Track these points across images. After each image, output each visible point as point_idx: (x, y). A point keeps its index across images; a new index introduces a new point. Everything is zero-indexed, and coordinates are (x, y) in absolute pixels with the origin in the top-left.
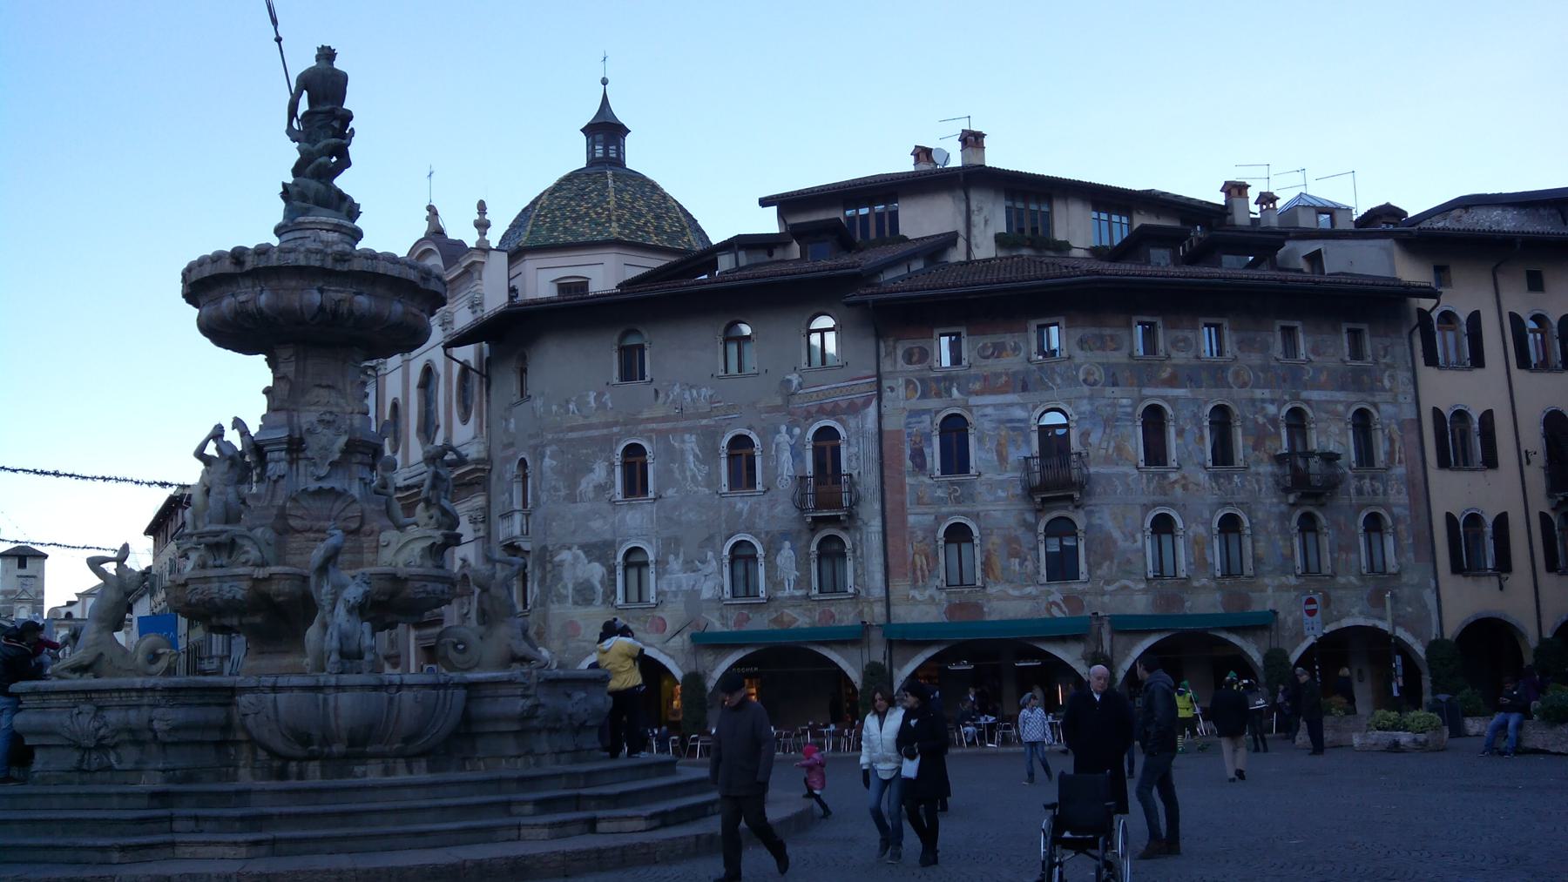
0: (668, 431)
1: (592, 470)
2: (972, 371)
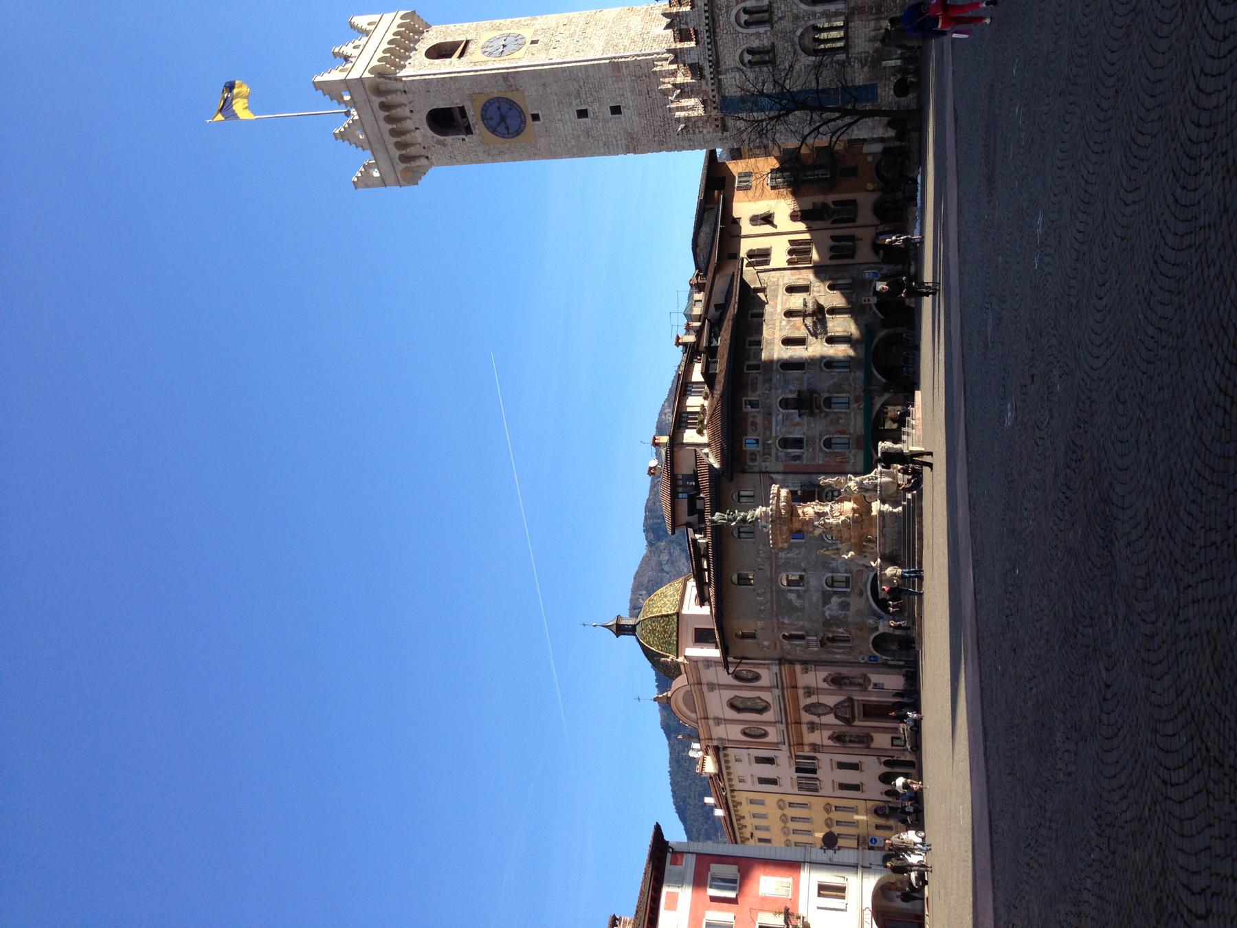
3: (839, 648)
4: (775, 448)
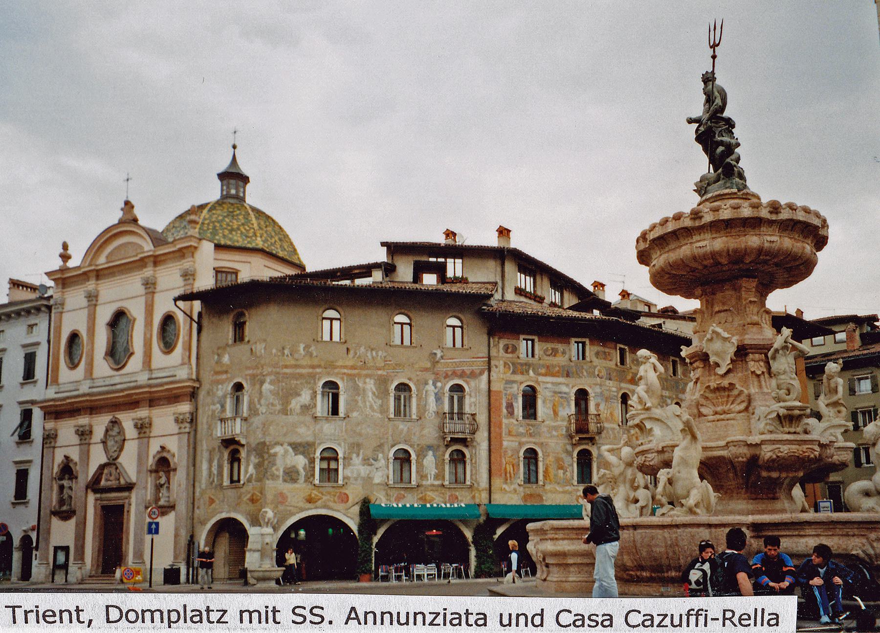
0: (355, 375)
1: (299, 395)
2: (541, 362)
3: (220, 467)
4: (529, 379)
